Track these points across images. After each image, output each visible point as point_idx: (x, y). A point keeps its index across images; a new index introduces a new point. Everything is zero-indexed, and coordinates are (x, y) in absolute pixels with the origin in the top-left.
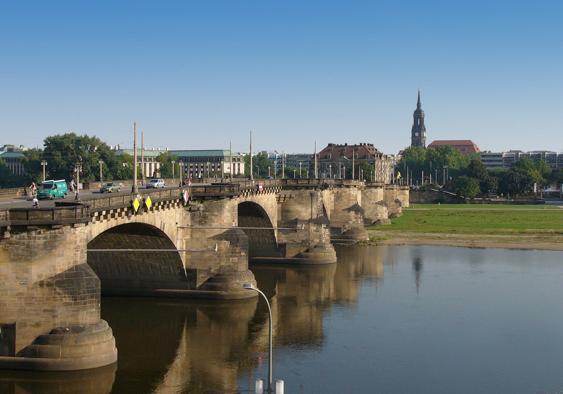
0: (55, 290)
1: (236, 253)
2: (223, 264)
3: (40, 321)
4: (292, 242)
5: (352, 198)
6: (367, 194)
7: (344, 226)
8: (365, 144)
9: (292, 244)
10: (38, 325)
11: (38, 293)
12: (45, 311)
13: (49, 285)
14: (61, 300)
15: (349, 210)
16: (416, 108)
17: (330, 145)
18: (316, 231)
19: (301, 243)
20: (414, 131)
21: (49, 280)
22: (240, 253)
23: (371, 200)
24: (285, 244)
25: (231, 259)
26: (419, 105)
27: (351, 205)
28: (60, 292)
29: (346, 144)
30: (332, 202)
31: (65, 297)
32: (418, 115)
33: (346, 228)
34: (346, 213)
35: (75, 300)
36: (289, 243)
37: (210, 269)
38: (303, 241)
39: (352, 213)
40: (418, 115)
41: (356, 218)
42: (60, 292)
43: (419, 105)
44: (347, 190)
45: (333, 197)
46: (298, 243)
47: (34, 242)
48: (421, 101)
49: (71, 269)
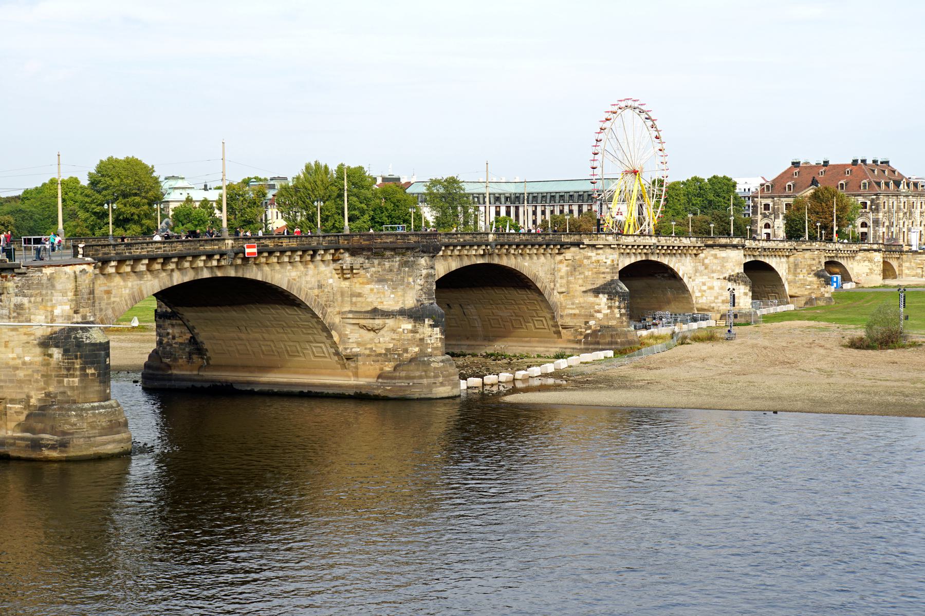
1: (75, 369)
2: (51, 389)
4: (367, 352)
5: (603, 269)
6: (706, 261)
7: (586, 323)
8: (864, 161)
9: (369, 356)
15: (597, 292)
17: (796, 164)
18: (414, 331)
19: (385, 355)
23: (713, 272)
24: (357, 355)
25: (66, 380)
27: (600, 282)
29: (826, 163)
30: (562, 278)
33: (590, 327)
34: (591, 298)
36: (364, 355)
37: (29, 397)
38: (387, 350)
39: (603, 298)
41: (610, 307)
44: (592, 253)
45: (564, 269)
46: (380, 355)
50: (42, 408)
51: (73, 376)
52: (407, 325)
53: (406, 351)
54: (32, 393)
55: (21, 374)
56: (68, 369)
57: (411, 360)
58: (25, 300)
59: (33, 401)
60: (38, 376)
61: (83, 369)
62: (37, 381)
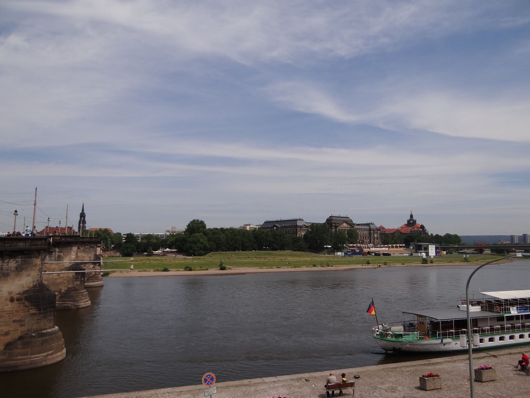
0: (24, 303)
2: (70, 286)
3: (9, 331)
10: (7, 334)
11: (9, 306)
12: (14, 321)
13: (18, 300)
14: (29, 311)
16: (81, 211)
20: (80, 223)
21: (18, 296)
22: (81, 278)
26: (83, 210)
28: (28, 305)
29: (57, 227)
31: (31, 309)
32: (83, 215)
35: (40, 310)
37: (61, 290)
40: (83, 215)
42: (28, 305)
43: (83, 210)
47: (8, 265)
48: (84, 208)
49: (35, 286)
50: (65, 293)
51: (78, 281)
52: (92, 266)
53: (91, 274)
54: (63, 288)
55: (58, 281)
56: (76, 279)
57: (92, 277)
58: (62, 254)
59: (63, 291)
60: (65, 282)
61: (81, 278)
62: (65, 284)
